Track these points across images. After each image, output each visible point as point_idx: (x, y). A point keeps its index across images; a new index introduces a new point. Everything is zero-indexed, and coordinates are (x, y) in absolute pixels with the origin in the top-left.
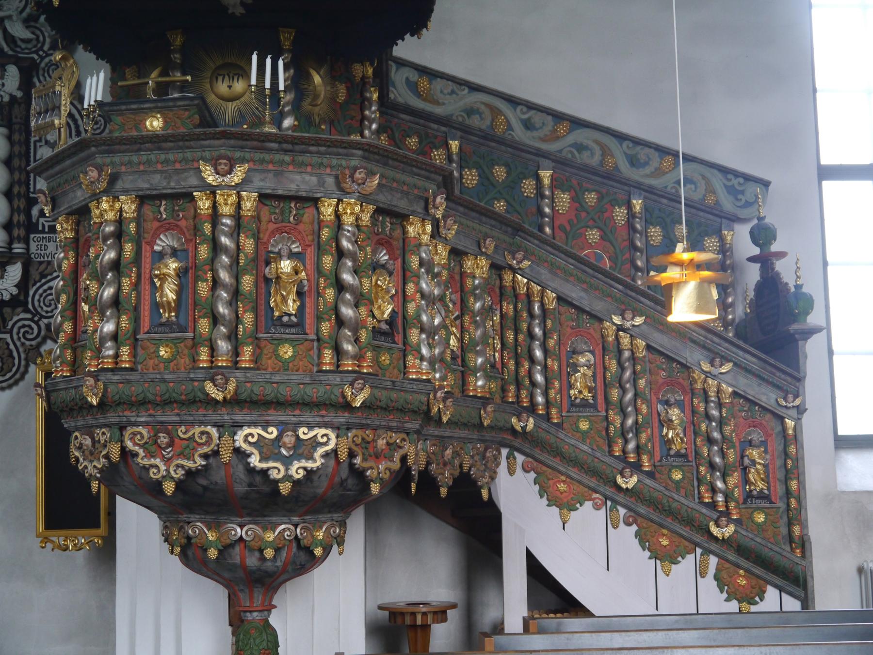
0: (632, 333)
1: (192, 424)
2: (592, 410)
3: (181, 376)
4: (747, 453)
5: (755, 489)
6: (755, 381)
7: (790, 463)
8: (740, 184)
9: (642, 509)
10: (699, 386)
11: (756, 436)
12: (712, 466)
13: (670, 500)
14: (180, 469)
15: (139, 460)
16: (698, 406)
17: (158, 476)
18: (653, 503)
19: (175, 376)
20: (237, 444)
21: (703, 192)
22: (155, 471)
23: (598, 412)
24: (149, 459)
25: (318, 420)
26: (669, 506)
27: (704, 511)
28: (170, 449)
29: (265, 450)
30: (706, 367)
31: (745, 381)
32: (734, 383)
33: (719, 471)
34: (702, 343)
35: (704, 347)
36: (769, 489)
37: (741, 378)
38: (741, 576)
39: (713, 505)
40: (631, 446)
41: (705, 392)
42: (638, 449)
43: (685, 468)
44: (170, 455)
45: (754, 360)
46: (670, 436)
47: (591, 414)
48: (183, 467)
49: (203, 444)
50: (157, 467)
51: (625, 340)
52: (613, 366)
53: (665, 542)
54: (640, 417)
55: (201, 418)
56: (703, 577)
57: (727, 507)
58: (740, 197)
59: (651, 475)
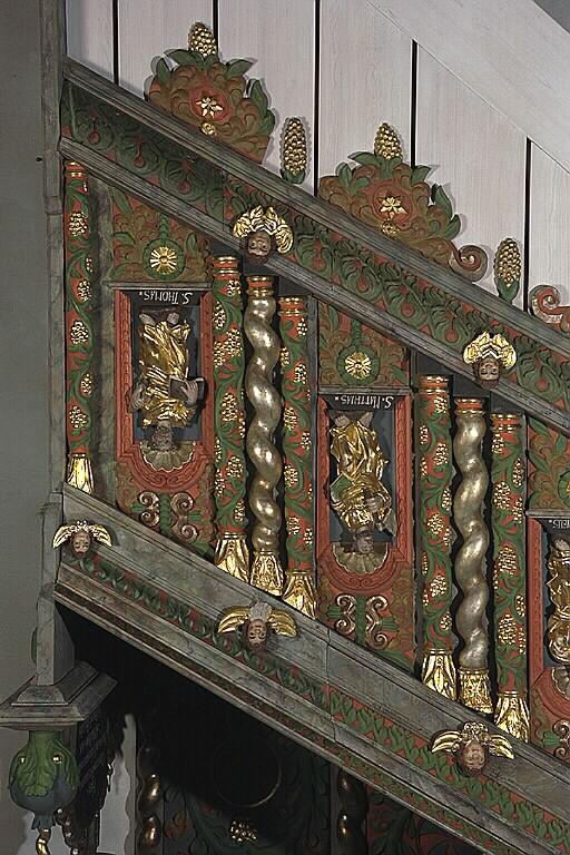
4: (185, 412)
5: (171, 326)
6: (163, 584)
7: (86, 385)
9: (447, 283)
18: (421, 295)
27: (303, 277)
36: (137, 326)
38: (211, 121)
39: (279, 287)
41: (284, 561)
45: (164, 640)
51: (475, 688)
52: (508, 631)
53: (390, 205)
54: (446, 502)
56: (295, 124)
57: (244, 286)
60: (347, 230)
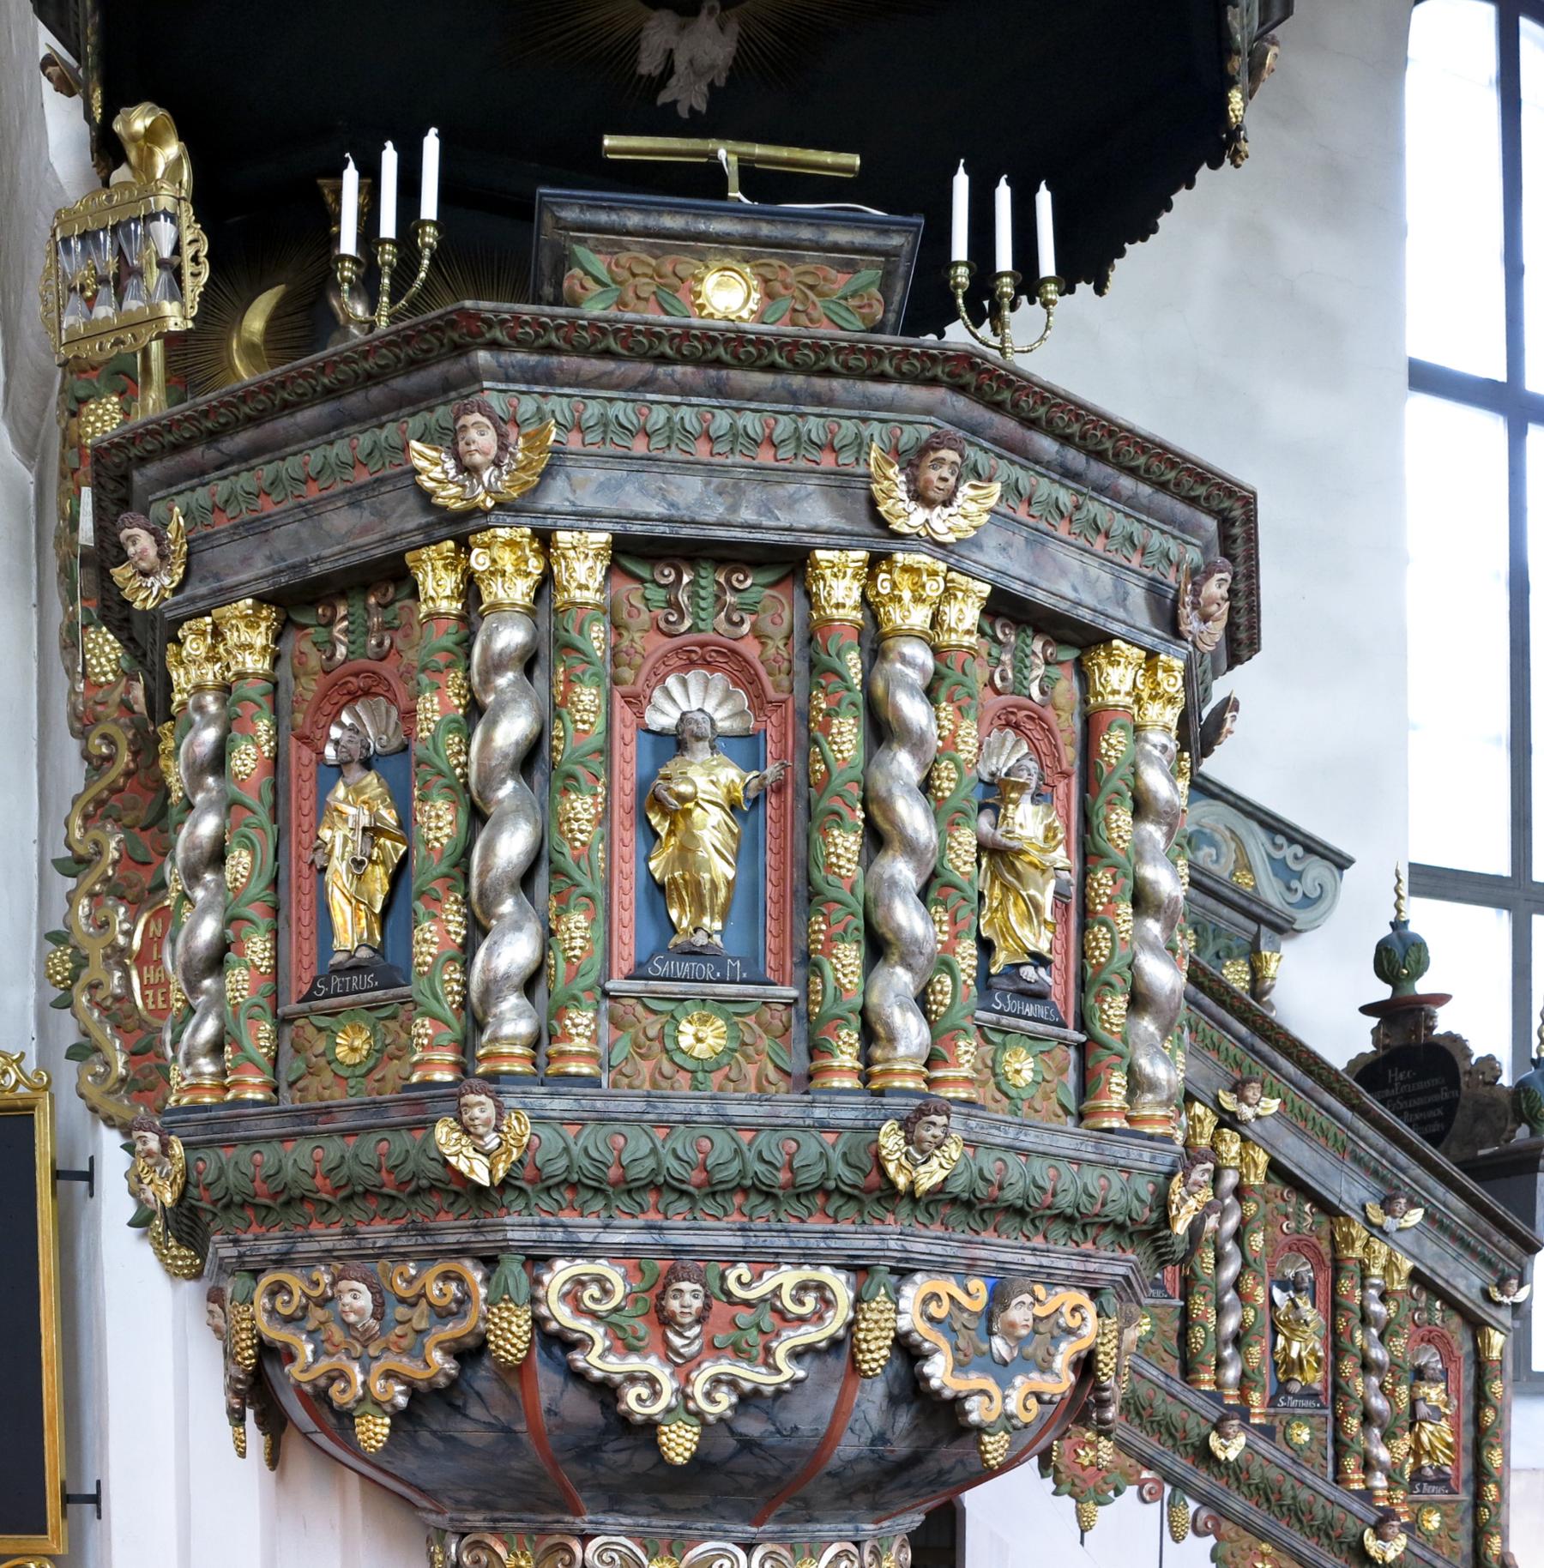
0: (1248, 1133)
1: (775, 1259)
2: (1159, 1292)
3: (783, 1111)
8: (1296, 857)
10: (1357, 1252)
11: (1430, 1358)
12: (1368, 1418)
13: (1297, 1484)
14: (724, 1389)
15: (593, 1358)
16: (1351, 1295)
17: (655, 1409)
18: (1265, 1494)
19: (765, 1109)
20: (904, 1323)
21: (1232, 867)
22: (645, 1392)
23: (1170, 1297)
24: (623, 1357)
25: (1075, 1265)
26: (1294, 1498)
28: (697, 1329)
29: (962, 1344)
30: (1376, 1215)
31: (1435, 1248)
32: (1415, 1251)
33: (1380, 1427)
34: (1372, 1163)
35: (1375, 1174)
37: (1429, 1243)
39: (1367, 1495)
40: (1231, 1374)
42: (1245, 1382)
43: (1315, 1421)
44: (695, 1347)
46: (1294, 1355)
47: (1158, 1302)
48: (733, 1383)
49: (802, 1320)
50: (651, 1380)
51: (1231, 1147)
55: (813, 1243)
58: (1295, 884)
59: (1267, 1432)
60: (1309, 1547)
